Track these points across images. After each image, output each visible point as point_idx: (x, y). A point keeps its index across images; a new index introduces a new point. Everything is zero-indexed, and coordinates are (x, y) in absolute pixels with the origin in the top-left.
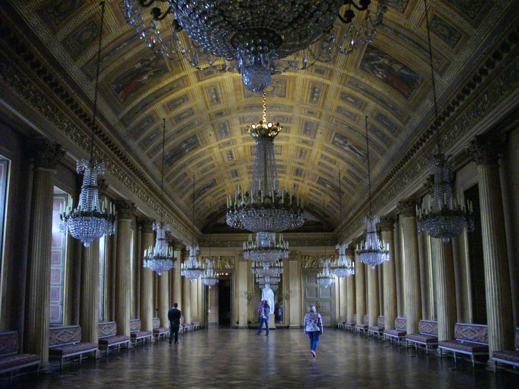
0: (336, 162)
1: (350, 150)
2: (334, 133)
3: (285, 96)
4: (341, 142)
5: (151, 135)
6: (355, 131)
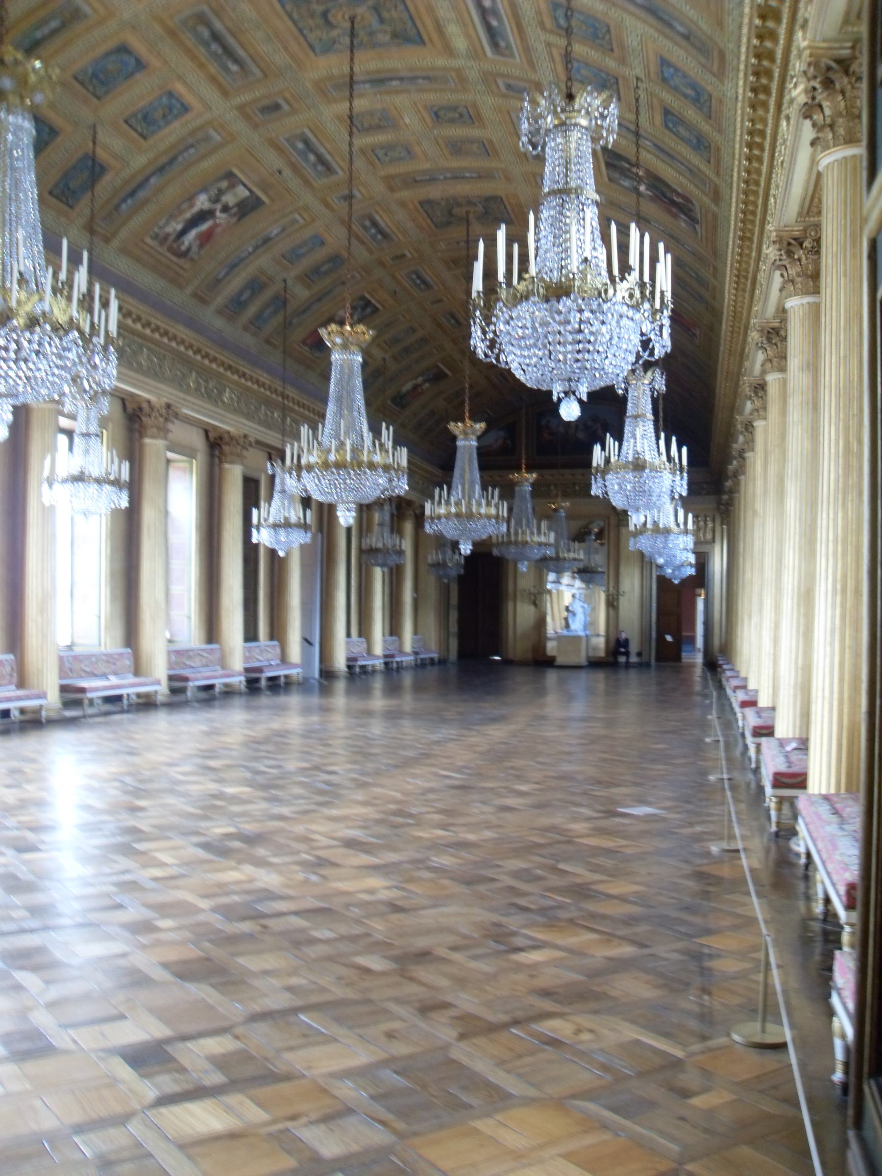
0: (144, 137)
1: (195, 210)
3: (421, 203)
4: (230, 199)
5: (692, 276)
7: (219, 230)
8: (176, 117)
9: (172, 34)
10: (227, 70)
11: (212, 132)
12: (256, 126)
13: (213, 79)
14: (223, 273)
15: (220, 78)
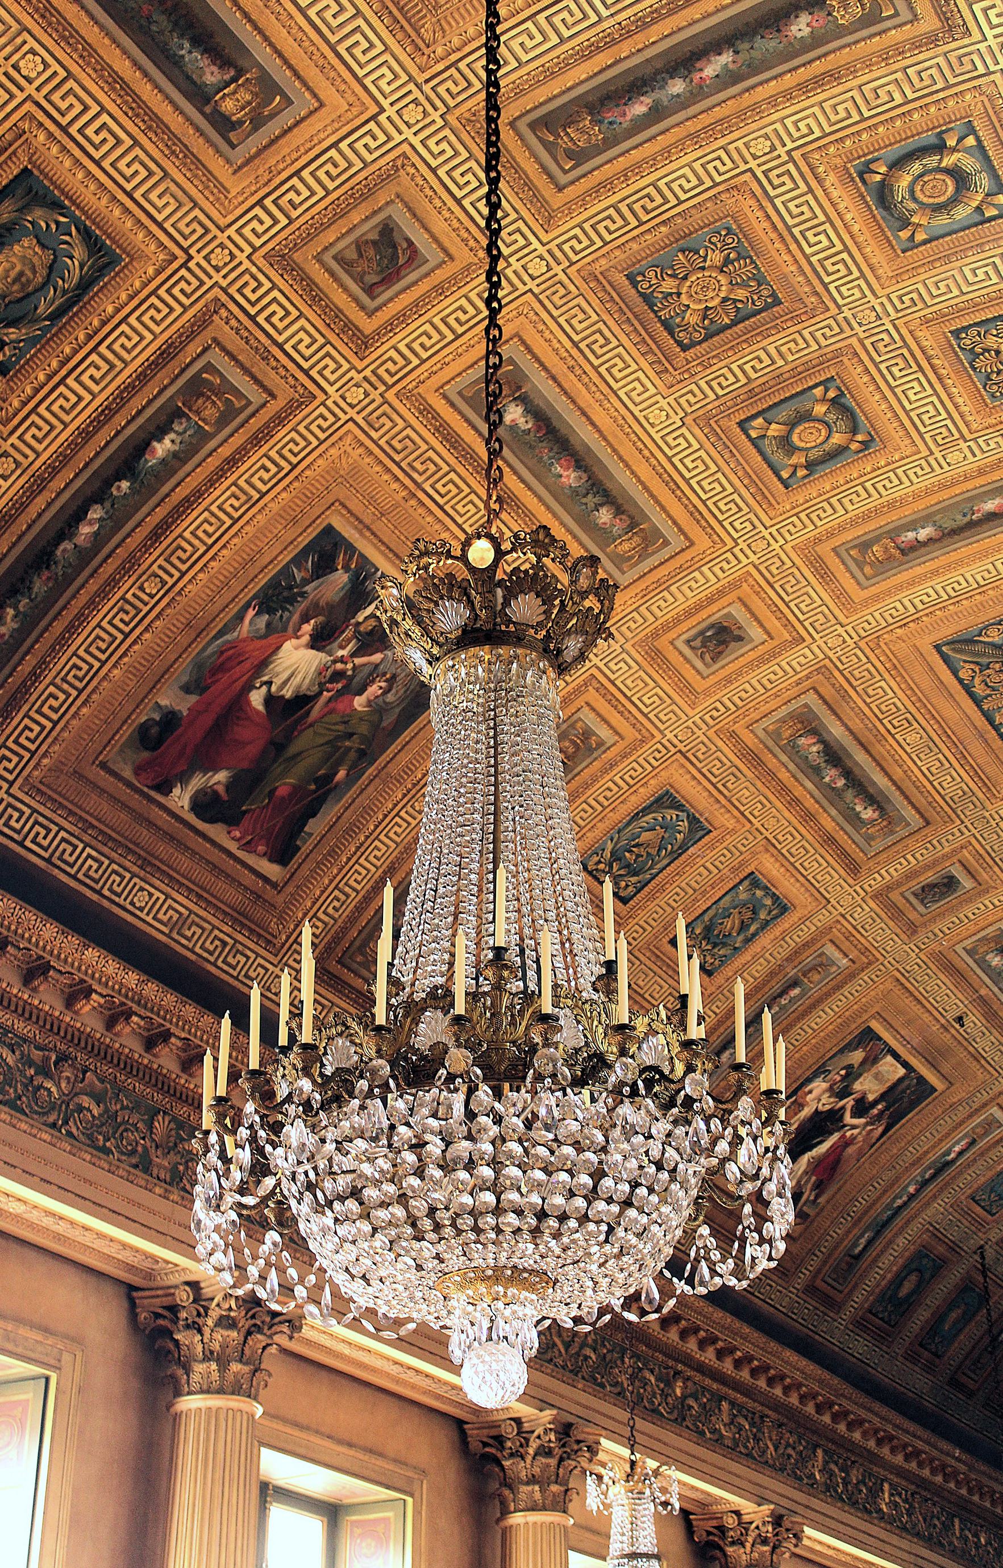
1: (806, 1112)
2: (932, 1078)
4: (868, 1086)
6: (925, 1183)
7: (850, 1150)
8: (765, 925)
9: (753, 759)
10: (854, 819)
11: (830, 950)
12: (912, 929)
13: (829, 840)
14: (863, 1241)
15: (841, 837)
